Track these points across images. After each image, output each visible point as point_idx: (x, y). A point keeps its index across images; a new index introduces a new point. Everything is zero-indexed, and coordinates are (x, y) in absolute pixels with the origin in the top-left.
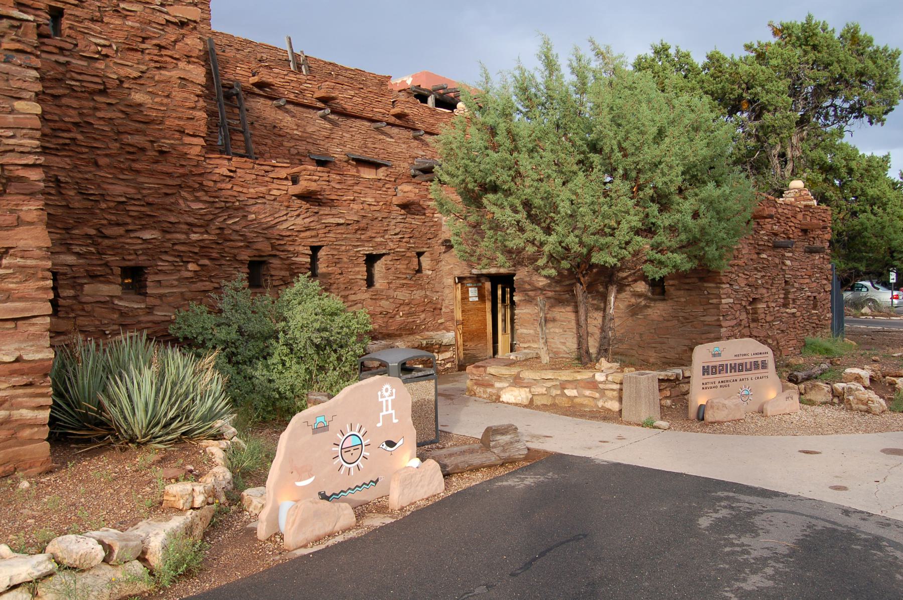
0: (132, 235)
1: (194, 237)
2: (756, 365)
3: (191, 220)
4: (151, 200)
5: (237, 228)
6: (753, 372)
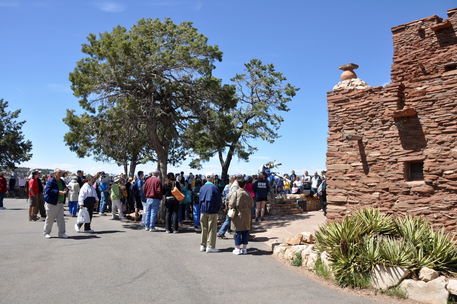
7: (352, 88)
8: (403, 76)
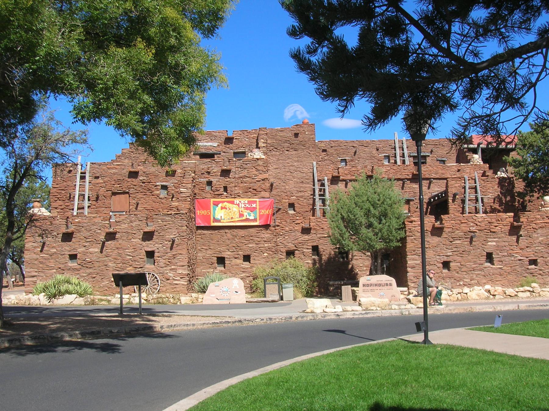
0: (246, 245)
1: (266, 245)
2: (387, 285)
3: (265, 240)
4: (252, 235)
5: (281, 241)
6: (385, 287)
7: (41, 214)
8: (58, 198)
